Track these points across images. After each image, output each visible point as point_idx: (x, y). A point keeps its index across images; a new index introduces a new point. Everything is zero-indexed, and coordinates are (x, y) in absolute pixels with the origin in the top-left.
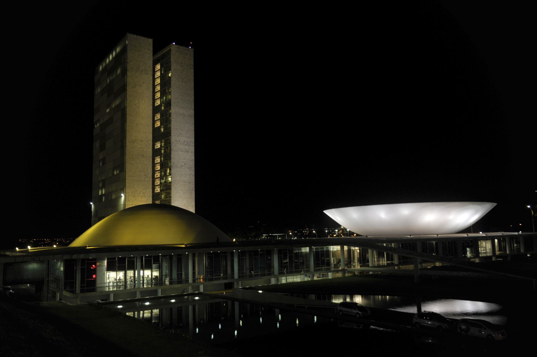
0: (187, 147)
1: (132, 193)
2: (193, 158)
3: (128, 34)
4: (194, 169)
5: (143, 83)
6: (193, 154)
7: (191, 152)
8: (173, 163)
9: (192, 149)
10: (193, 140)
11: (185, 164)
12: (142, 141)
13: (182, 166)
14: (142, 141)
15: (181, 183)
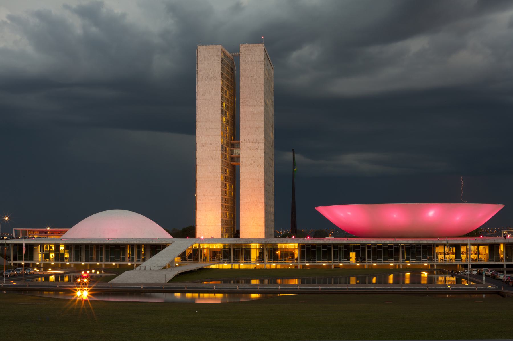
0: (256, 145)
1: (202, 192)
2: (263, 154)
3: (198, 47)
4: (264, 166)
5: (212, 89)
6: (263, 151)
7: (261, 149)
8: (242, 162)
9: (262, 146)
10: (263, 137)
11: (254, 162)
12: (211, 144)
13: (251, 164)
14: (211, 144)
15: (250, 181)
